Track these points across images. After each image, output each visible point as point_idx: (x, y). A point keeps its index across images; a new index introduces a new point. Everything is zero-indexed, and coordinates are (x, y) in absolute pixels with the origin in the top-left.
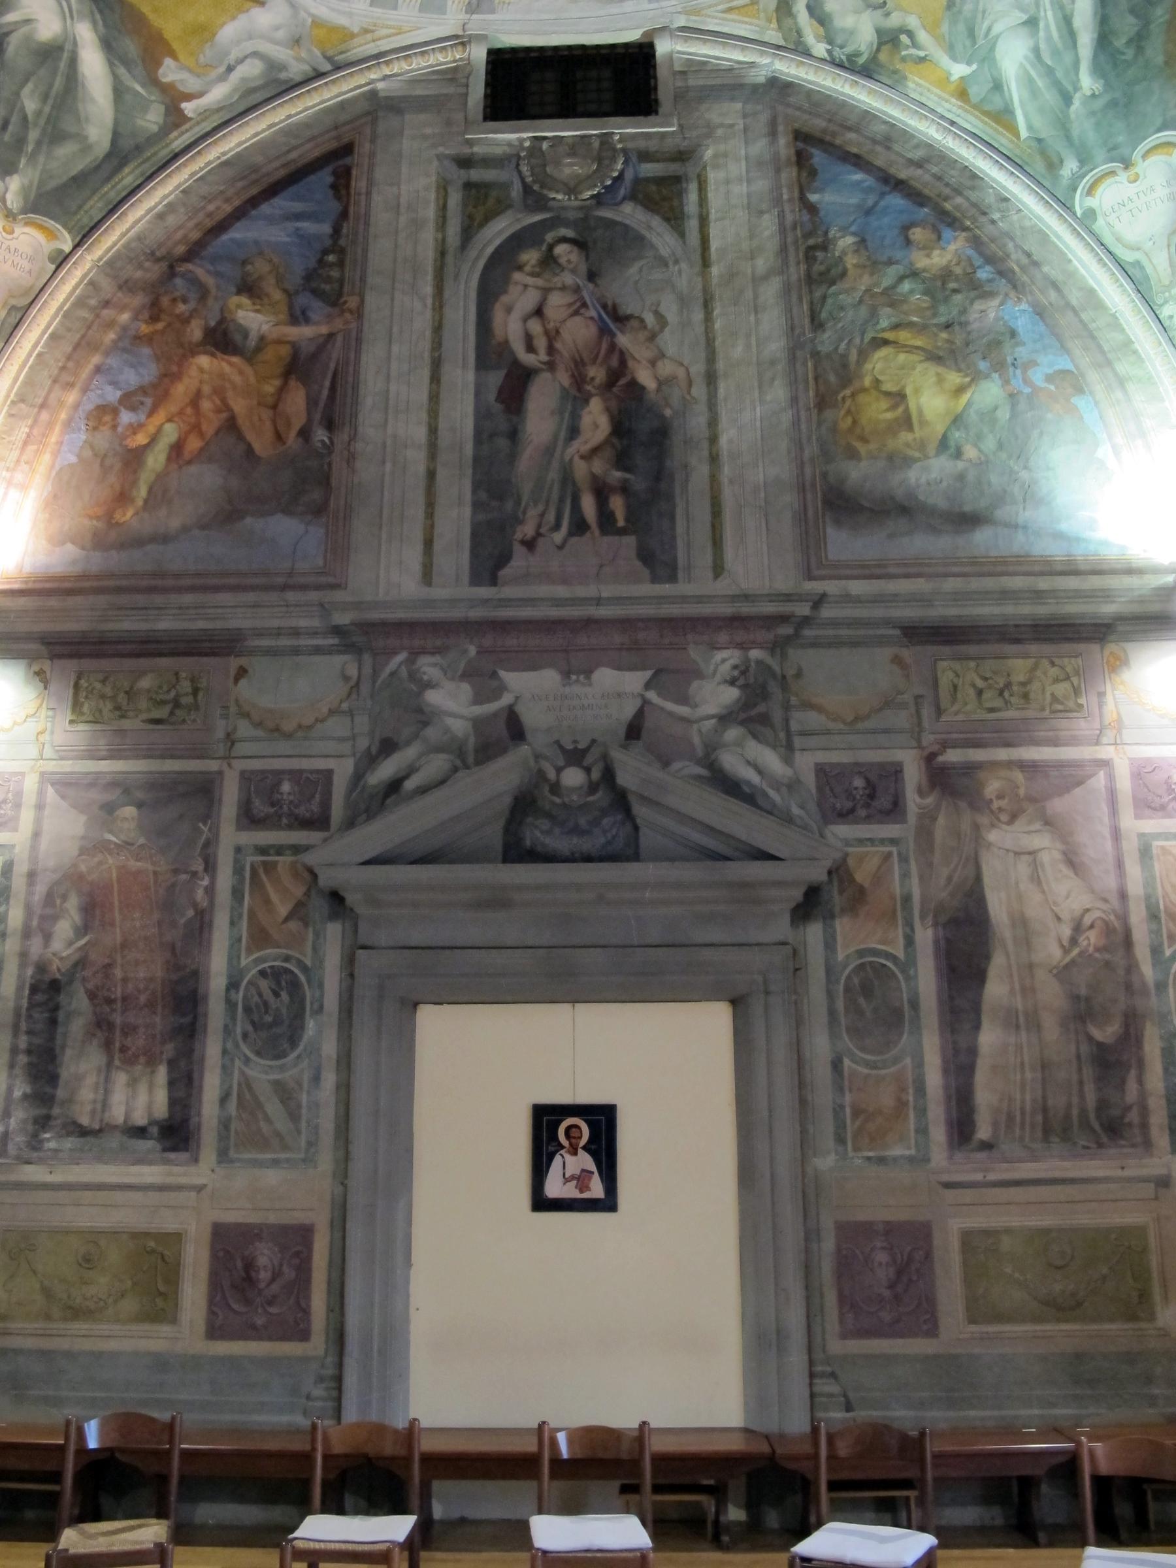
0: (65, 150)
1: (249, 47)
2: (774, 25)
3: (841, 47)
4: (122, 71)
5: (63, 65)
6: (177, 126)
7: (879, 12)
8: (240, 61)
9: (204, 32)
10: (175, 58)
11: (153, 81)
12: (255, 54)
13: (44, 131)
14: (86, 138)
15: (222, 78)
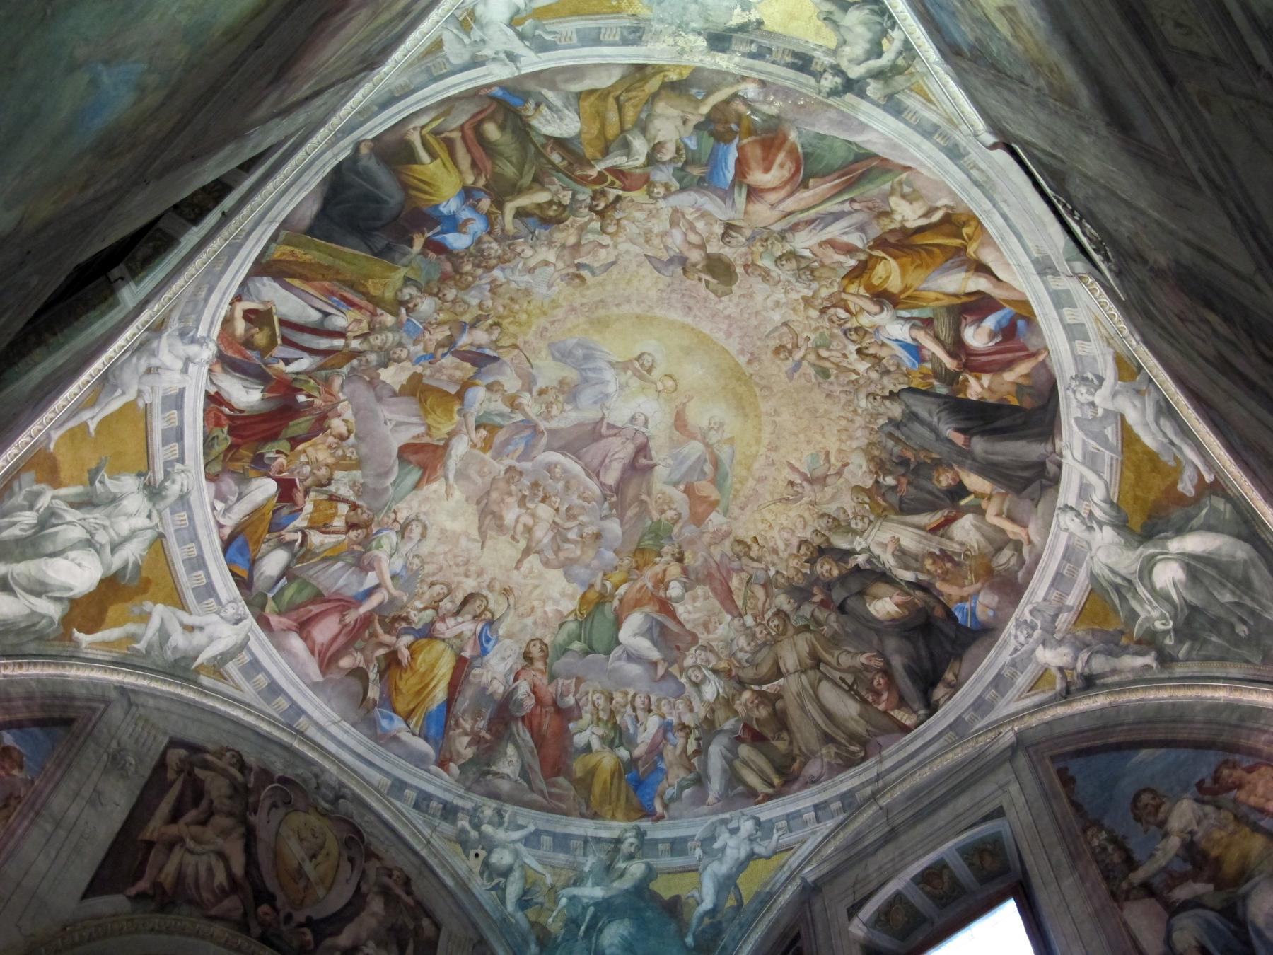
0: (1257, 583)
1: (1153, 426)
2: (912, 69)
3: (881, 24)
4: (1195, 522)
5: (1199, 566)
6: (1224, 490)
7: (835, 17)
8: (1165, 435)
9: (1152, 457)
10: (1175, 484)
11: (1197, 501)
12: (1157, 423)
13: (1246, 594)
14: (1245, 561)
15: (1180, 450)
